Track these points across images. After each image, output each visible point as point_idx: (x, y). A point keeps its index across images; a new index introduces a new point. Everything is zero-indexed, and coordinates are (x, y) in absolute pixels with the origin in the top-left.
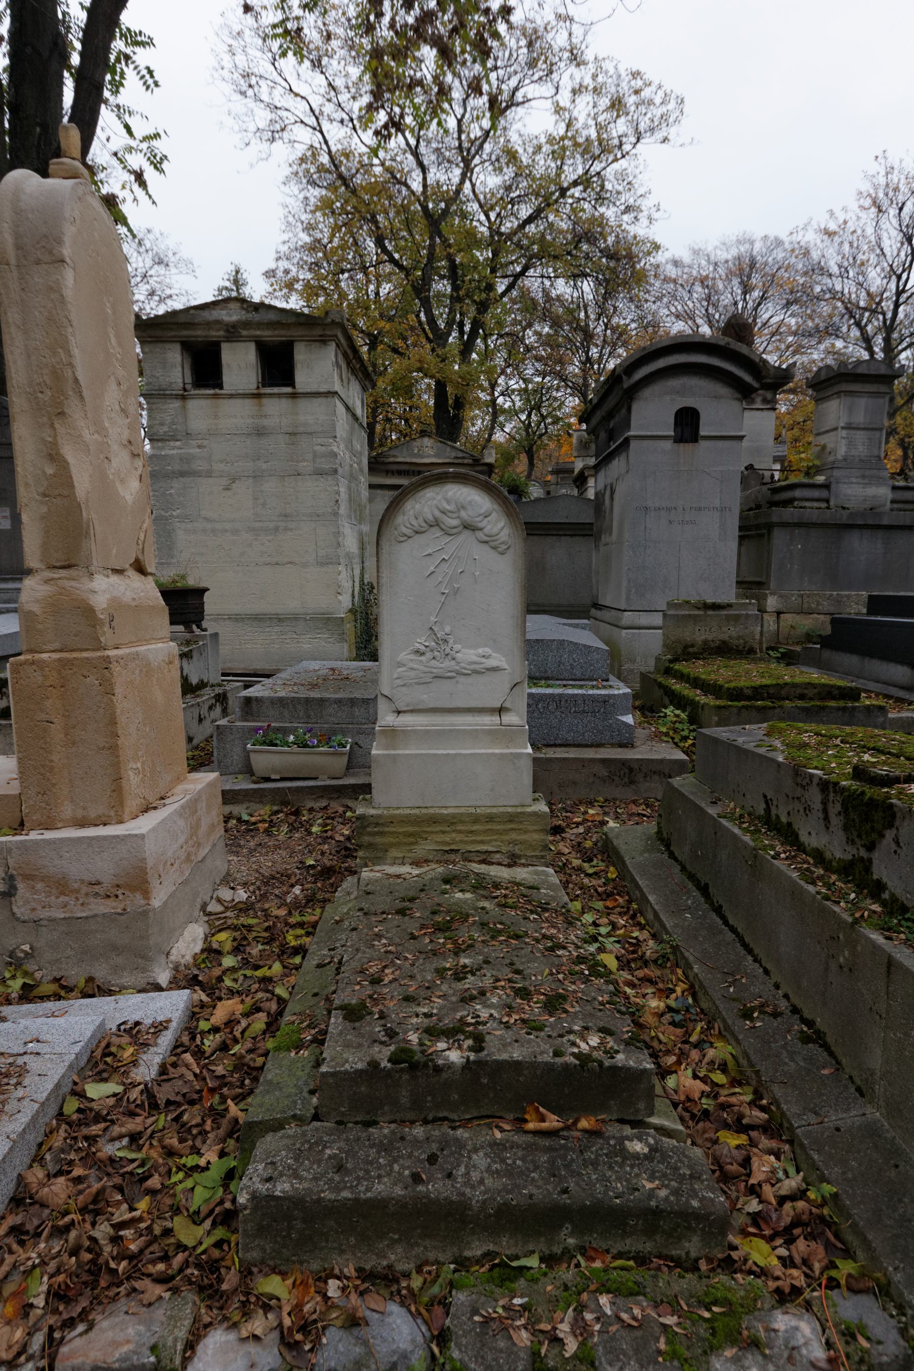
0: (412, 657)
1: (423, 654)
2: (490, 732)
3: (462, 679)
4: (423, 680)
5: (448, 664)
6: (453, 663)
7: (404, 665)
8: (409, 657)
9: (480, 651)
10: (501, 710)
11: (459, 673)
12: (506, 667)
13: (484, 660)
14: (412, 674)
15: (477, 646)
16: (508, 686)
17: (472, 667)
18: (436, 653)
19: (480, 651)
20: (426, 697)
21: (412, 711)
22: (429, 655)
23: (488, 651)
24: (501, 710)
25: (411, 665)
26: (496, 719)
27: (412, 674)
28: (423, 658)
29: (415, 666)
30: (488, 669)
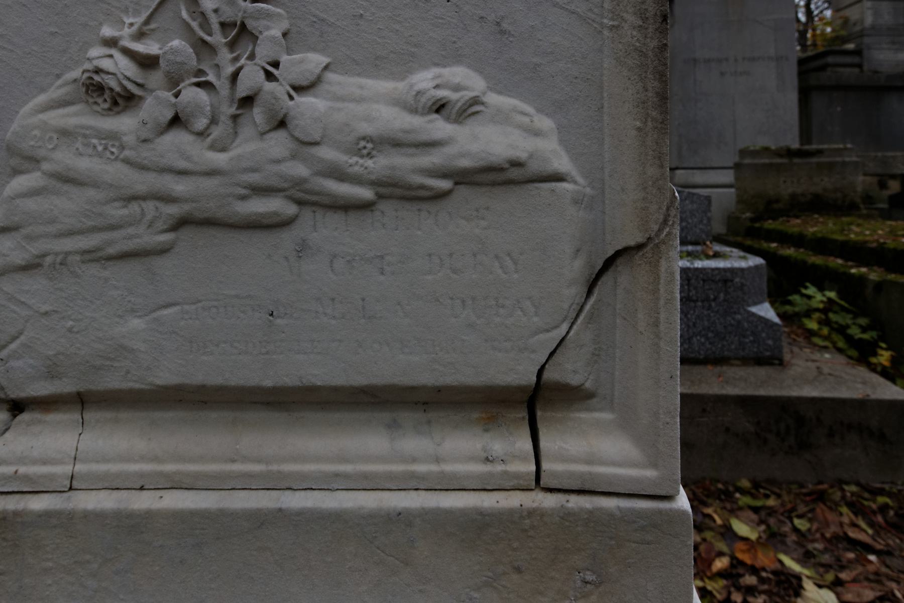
0: (77, 117)
1: (124, 100)
2: (476, 528)
3: (326, 231)
4: (120, 242)
5: (255, 149)
6: (277, 144)
7: (34, 161)
8: (56, 118)
9: (424, 80)
10: (535, 402)
11: (309, 200)
12: (562, 163)
13: (440, 127)
14: (68, 205)
15: (403, 63)
16: (576, 269)
17: (380, 164)
18: (191, 95)
19: (424, 80)
20: (134, 325)
21: (81, 401)
22: (156, 105)
23: (464, 79)
24: (535, 402)
25: (65, 158)
26: (510, 447)
27: (68, 205)
28: (125, 124)
29: (85, 164)
30: (464, 178)
